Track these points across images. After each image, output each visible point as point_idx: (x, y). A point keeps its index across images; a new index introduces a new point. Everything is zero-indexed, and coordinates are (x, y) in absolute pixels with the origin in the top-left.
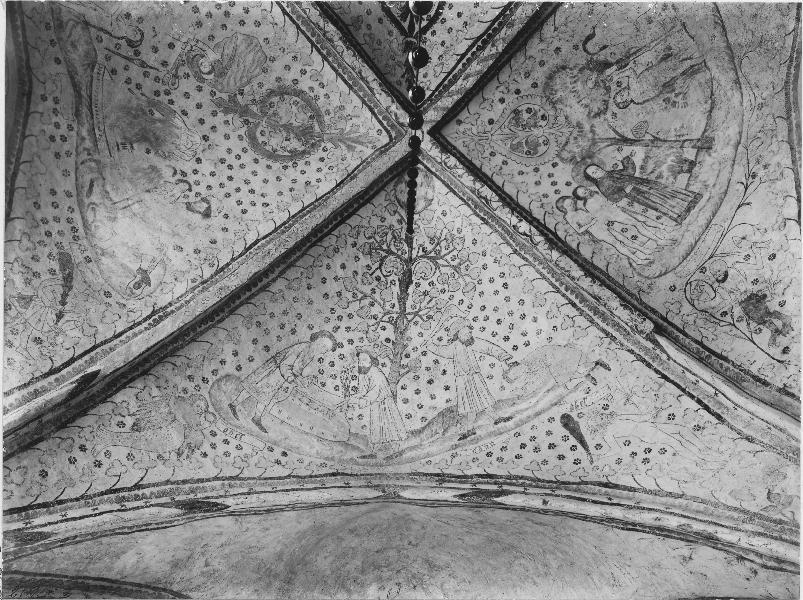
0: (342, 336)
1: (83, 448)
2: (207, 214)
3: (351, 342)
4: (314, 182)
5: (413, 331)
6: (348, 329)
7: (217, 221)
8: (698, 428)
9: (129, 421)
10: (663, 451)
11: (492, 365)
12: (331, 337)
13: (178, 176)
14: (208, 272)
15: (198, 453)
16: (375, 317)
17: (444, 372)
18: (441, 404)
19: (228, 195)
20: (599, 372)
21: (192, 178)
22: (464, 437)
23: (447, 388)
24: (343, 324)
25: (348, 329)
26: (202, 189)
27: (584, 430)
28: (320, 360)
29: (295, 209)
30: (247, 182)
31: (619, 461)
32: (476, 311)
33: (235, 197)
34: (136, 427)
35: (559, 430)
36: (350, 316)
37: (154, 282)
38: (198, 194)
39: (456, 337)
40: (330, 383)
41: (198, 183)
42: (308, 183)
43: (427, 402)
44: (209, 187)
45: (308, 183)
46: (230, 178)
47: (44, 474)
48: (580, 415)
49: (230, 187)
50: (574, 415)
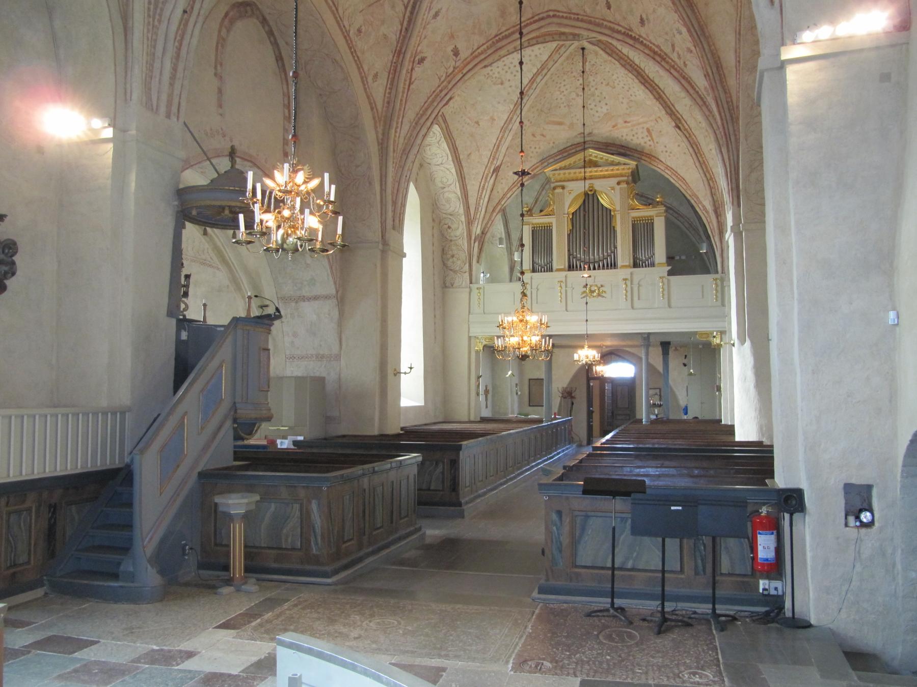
0: (562, 89)
1: (502, 179)
2: (502, 84)
3: (567, 90)
4: (539, 55)
5: (591, 79)
6: (564, 85)
7: (507, 84)
8: (685, 153)
9: (509, 164)
10: (674, 156)
11: (623, 98)
12: (560, 91)
13: (487, 76)
14: (512, 107)
15: (529, 158)
16: (574, 77)
17: (605, 98)
18: (605, 111)
19: (507, 72)
20: (659, 120)
21: (491, 73)
22: (614, 127)
23: (606, 104)
24: (562, 85)
25: (564, 85)
26: (496, 75)
27: (654, 136)
28: (557, 99)
29: (535, 71)
30: (512, 63)
31: (662, 152)
32: (614, 77)
33: (509, 71)
34: (511, 165)
35: (645, 130)
36: (564, 80)
37: (495, 118)
38: (496, 77)
39: (608, 84)
40: (562, 105)
41: (494, 74)
42: (536, 56)
43: (599, 109)
44: (499, 73)
45: (536, 56)
46: (505, 65)
47: (498, 192)
48: (653, 130)
49: (506, 68)
50: (651, 129)
